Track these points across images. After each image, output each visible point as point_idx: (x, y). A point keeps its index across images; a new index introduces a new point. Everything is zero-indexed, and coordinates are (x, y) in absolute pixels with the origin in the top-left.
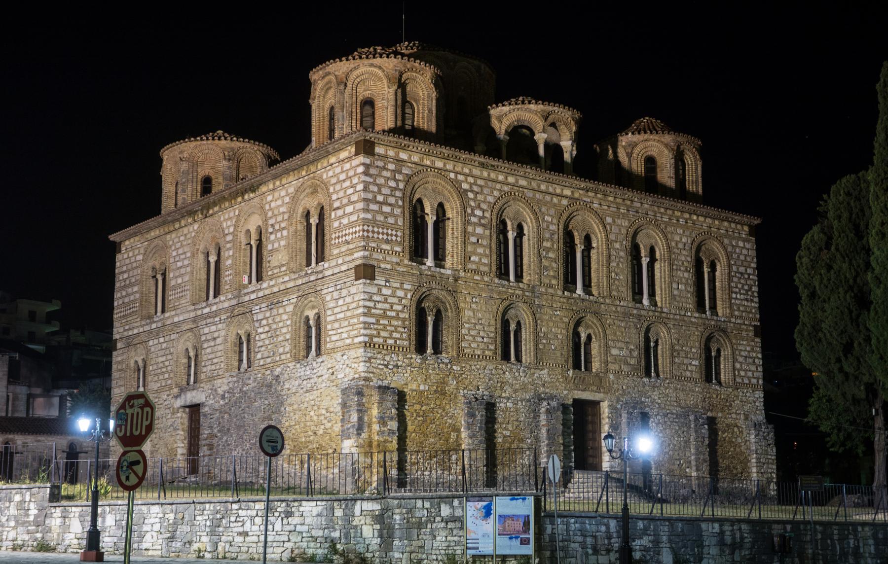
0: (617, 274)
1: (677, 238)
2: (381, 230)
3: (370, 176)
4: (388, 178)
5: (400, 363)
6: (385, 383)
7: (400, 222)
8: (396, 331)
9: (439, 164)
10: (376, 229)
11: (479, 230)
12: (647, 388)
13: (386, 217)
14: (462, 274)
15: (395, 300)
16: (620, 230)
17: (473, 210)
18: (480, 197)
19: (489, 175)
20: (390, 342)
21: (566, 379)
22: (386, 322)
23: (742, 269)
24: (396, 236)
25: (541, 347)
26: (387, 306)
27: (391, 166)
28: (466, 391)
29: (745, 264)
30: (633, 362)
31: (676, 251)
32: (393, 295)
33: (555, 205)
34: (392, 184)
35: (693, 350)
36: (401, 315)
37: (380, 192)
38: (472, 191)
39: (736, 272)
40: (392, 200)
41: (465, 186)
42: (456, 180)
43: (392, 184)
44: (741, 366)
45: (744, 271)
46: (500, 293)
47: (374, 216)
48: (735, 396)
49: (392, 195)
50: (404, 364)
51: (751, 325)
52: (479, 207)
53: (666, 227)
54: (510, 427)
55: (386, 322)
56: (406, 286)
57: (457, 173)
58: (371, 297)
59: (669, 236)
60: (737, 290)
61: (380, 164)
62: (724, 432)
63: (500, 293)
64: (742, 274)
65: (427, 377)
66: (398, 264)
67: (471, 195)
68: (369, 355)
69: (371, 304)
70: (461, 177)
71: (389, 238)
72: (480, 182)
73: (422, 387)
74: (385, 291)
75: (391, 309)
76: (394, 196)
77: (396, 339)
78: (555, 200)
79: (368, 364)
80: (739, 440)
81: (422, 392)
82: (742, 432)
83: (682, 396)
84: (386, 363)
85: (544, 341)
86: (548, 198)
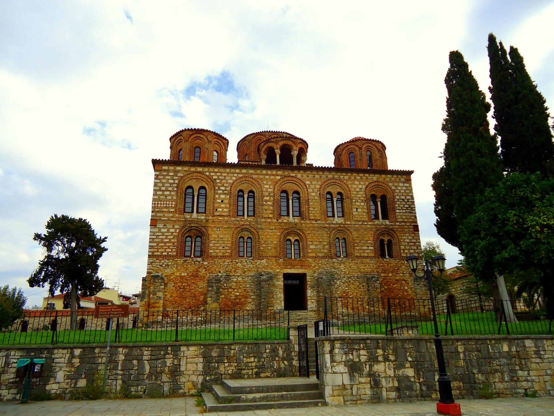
0: (314, 208)
1: (356, 186)
2: (162, 203)
3: (159, 179)
4: (169, 179)
5: (170, 263)
6: (160, 274)
7: (175, 198)
8: (169, 248)
9: (200, 169)
10: (159, 203)
11: (223, 196)
12: (336, 264)
13: (166, 197)
14: (210, 218)
15: (170, 234)
16: (315, 187)
17: (219, 187)
18: (223, 181)
19: (230, 171)
20: (166, 253)
21: (279, 265)
22: (163, 245)
23: (403, 197)
24: (172, 204)
25: (262, 248)
26: (164, 237)
27: (171, 174)
28: (211, 274)
29: (404, 194)
30: (326, 251)
31: (354, 193)
32: (168, 231)
33: (273, 179)
34: (172, 181)
35: (369, 242)
36: (172, 241)
37: (163, 186)
38: (219, 179)
39: (398, 199)
40: (170, 189)
41: (214, 177)
42: (210, 175)
43: (172, 181)
44: (405, 247)
45: (404, 198)
46: (234, 225)
47: (159, 197)
48: (401, 263)
49: (170, 186)
50: (173, 263)
51: (411, 225)
52: (223, 186)
53: (347, 182)
54: (240, 291)
55: (163, 245)
56: (175, 227)
57: (210, 172)
58: (154, 234)
59: (350, 186)
60: (400, 208)
61: (165, 173)
62: (394, 285)
63: (234, 225)
64: (403, 200)
65: (187, 269)
66: (172, 217)
67: (218, 181)
68: (151, 261)
69: (155, 237)
70: (212, 174)
71: (168, 205)
72: (224, 174)
73: (183, 274)
74: (163, 230)
75: (167, 238)
76: (172, 187)
77: (168, 252)
78: (272, 177)
79: (151, 266)
80: (406, 288)
81: (182, 277)
82: (408, 283)
83: (362, 267)
84: (161, 264)
85: (264, 245)
86: (267, 177)
